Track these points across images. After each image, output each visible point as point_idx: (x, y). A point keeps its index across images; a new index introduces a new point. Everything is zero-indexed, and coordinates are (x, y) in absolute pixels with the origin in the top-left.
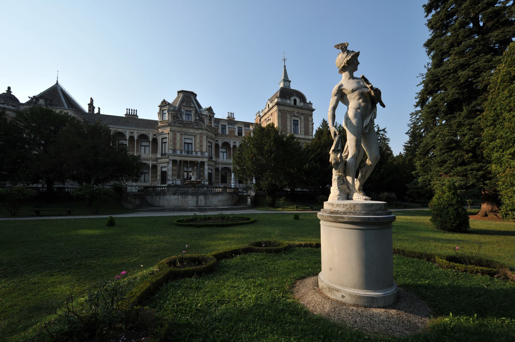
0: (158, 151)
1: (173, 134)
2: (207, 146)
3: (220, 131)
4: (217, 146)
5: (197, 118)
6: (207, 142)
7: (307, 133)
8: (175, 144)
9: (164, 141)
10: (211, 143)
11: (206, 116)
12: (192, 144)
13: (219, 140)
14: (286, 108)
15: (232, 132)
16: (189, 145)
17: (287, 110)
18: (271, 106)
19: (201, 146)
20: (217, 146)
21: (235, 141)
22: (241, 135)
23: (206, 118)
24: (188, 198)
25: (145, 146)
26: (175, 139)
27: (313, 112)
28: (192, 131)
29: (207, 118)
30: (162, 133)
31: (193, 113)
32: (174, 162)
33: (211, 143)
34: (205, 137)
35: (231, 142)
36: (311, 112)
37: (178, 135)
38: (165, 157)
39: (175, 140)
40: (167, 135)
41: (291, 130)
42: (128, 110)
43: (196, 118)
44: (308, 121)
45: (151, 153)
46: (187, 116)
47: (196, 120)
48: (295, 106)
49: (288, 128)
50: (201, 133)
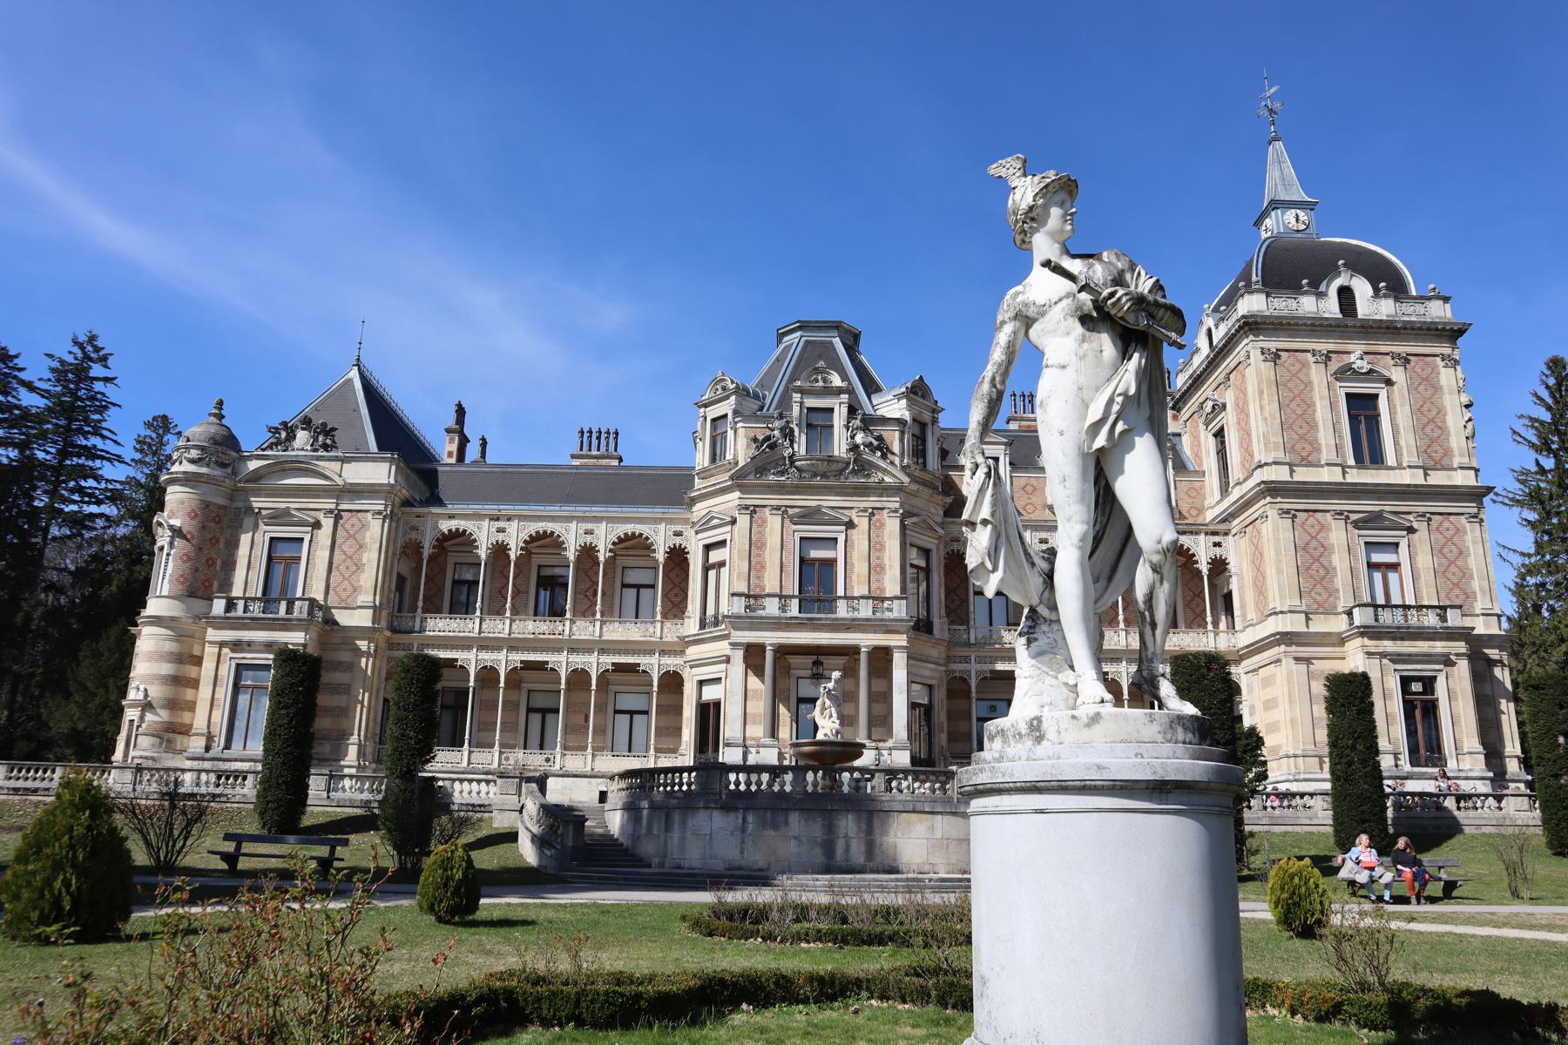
0: (690, 607)
5: (859, 438)
7: (1437, 457)
8: (755, 566)
9: (715, 556)
11: (900, 422)
12: (835, 560)
15: (1029, 488)
18: (1218, 335)
19: (874, 569)
24: (787, 823)
25: (638, 587)
26: (755, 545)
31: (839, 418)
32: (753, 655)
34: (892, 526)
37: (774, 522)
39: (758, 548)
40: (728, 528)
41: (1338, 448)
44: (1437, 388)
45: (659, 617)
47: (854, 448)
48: (1350, 321)
49: (1322, 441)
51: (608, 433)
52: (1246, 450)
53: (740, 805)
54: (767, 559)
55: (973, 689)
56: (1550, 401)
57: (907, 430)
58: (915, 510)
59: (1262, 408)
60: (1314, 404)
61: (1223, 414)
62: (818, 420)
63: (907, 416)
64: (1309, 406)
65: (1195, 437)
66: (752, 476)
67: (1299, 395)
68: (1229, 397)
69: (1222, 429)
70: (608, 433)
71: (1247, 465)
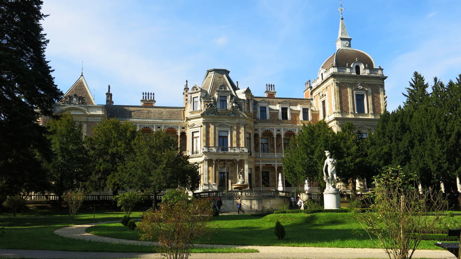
1: (206, 127)
3: (259, 115)
4: (256, 136)
5: (234, 105)
9: (195, 135)
10: (250, 134)
13: (259, 129)
14: (346, 79)
15: (274, 115)
16: (224, 138)
17: (347, 82)
18: (325, 76)
20: (256, 136)
21: (278, 128)
22: (286, 118)
23: (243, 103)
26: (207, 132)
27: (385, 81)
28: (227, 121)
29: (244, 103)
30: (193, 126)
33: (250, 134)
35: (273, 130)
36: (381, 81)
37: (212, 127)
38: (197, 155)
40: (200, 128)
42: (144, 94)
43: (232, 104)
46: (222, 102)
47: (233, 107)
48: (358, 75)
49: (350, 107)
51: (151, 94)
52: (331, 108)
55: (261, 169)
56: (414, 84)
57: (245, 102)
58: (247, 123)
59: (335, 98)
60: (348, 97)
61: (325, 97)
62: (223, 99)
63: (245, 98)
64: (347, 98)
65: (317, 101)
66: (206, 115)
67: (344, 95)
68: (326, 93)
69: (324, 101)
70: (151, 94)
71: (331, 112)
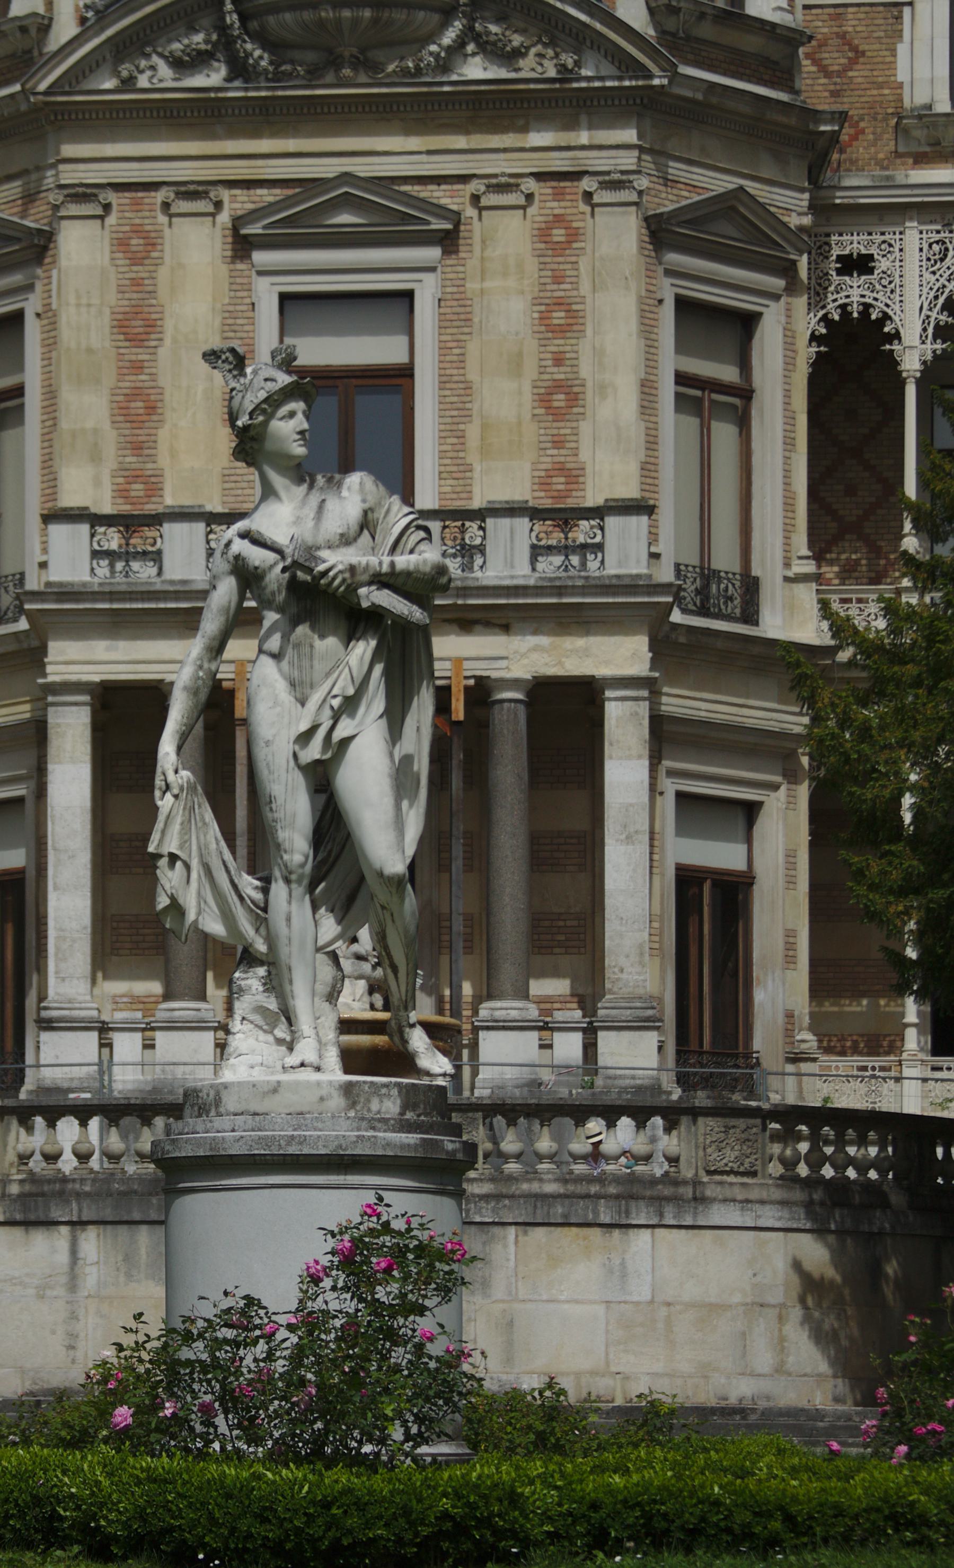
1: (121, 244)
2: (647, 388)
6: (647, 329)
39: (137, 340)
50: (558, 162)
53: (56, 1213)
54: (164, 380)
